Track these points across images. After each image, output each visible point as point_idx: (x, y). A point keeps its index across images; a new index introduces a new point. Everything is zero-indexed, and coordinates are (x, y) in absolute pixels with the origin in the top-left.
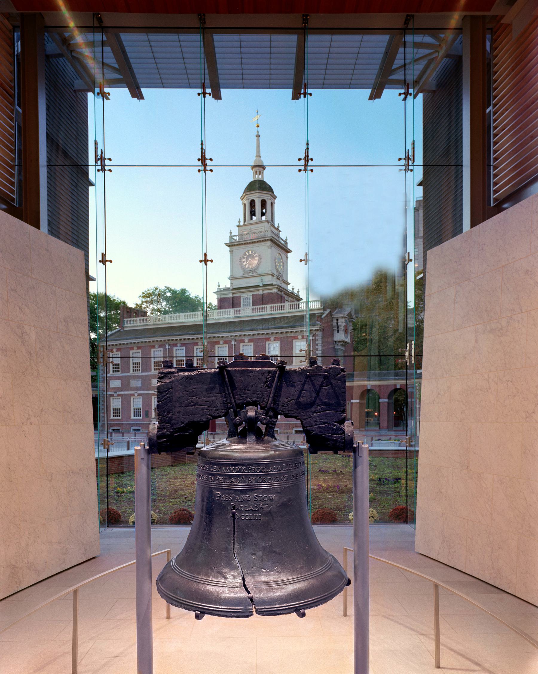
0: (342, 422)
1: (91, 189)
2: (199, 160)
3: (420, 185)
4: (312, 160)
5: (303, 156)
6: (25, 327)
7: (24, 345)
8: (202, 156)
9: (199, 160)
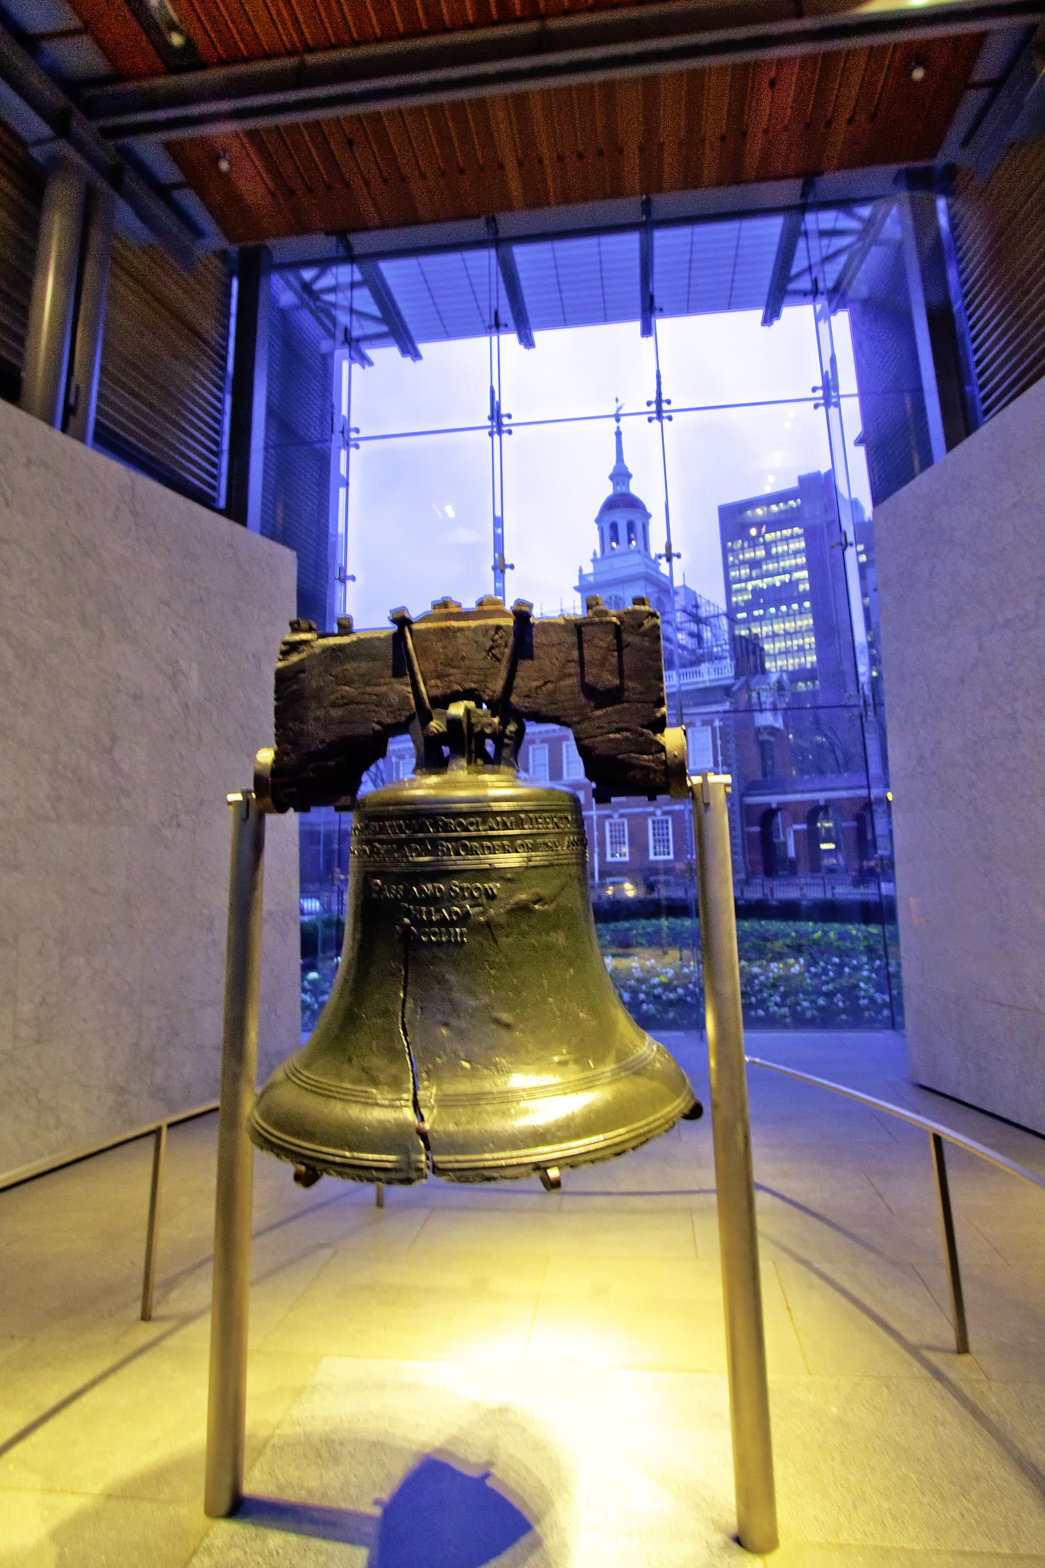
0: (660, 726)
6: (181, 662)
7: (176, 691)
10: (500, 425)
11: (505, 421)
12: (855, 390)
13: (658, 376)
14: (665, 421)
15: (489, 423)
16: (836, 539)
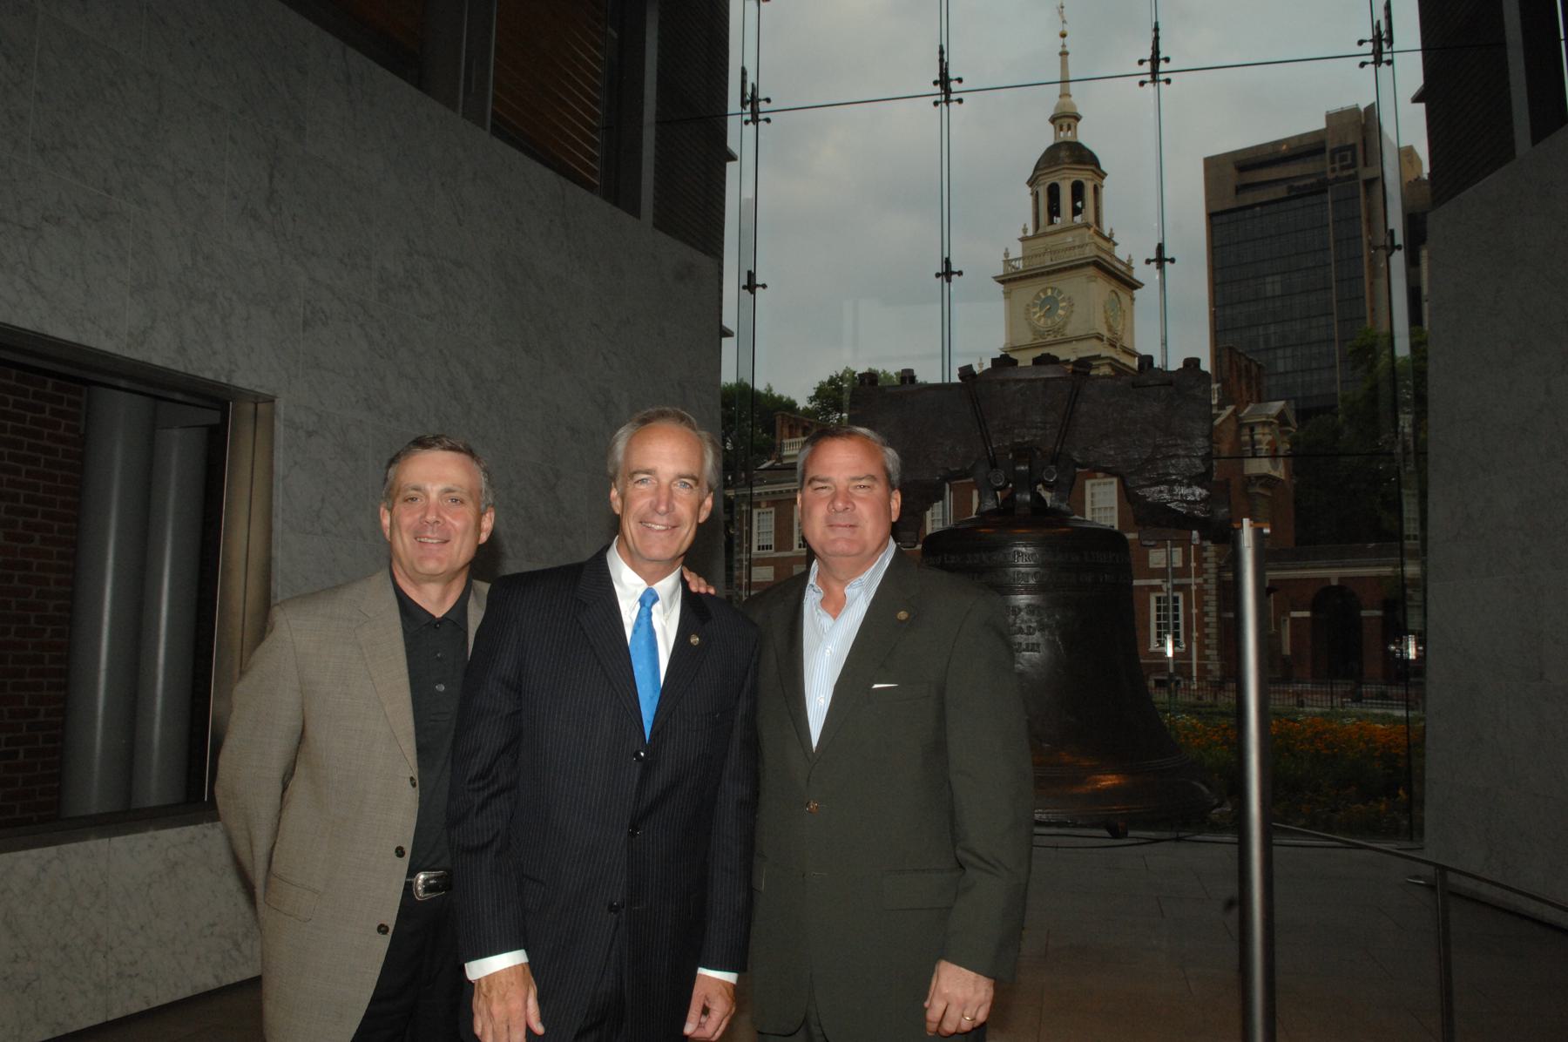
1: (731, 167)
2: (935, 83)
3: (1416, 99)
4: (1167, 60)
5: (1148, 54)
8: (941, 74)
9: (935, 83)
10: (947, 91)
11: (954, 86)
12: (1416, 42)
13: (1156, 29)
14: (1163, 84)
15: (938, 89)
16: (1382, 239)
